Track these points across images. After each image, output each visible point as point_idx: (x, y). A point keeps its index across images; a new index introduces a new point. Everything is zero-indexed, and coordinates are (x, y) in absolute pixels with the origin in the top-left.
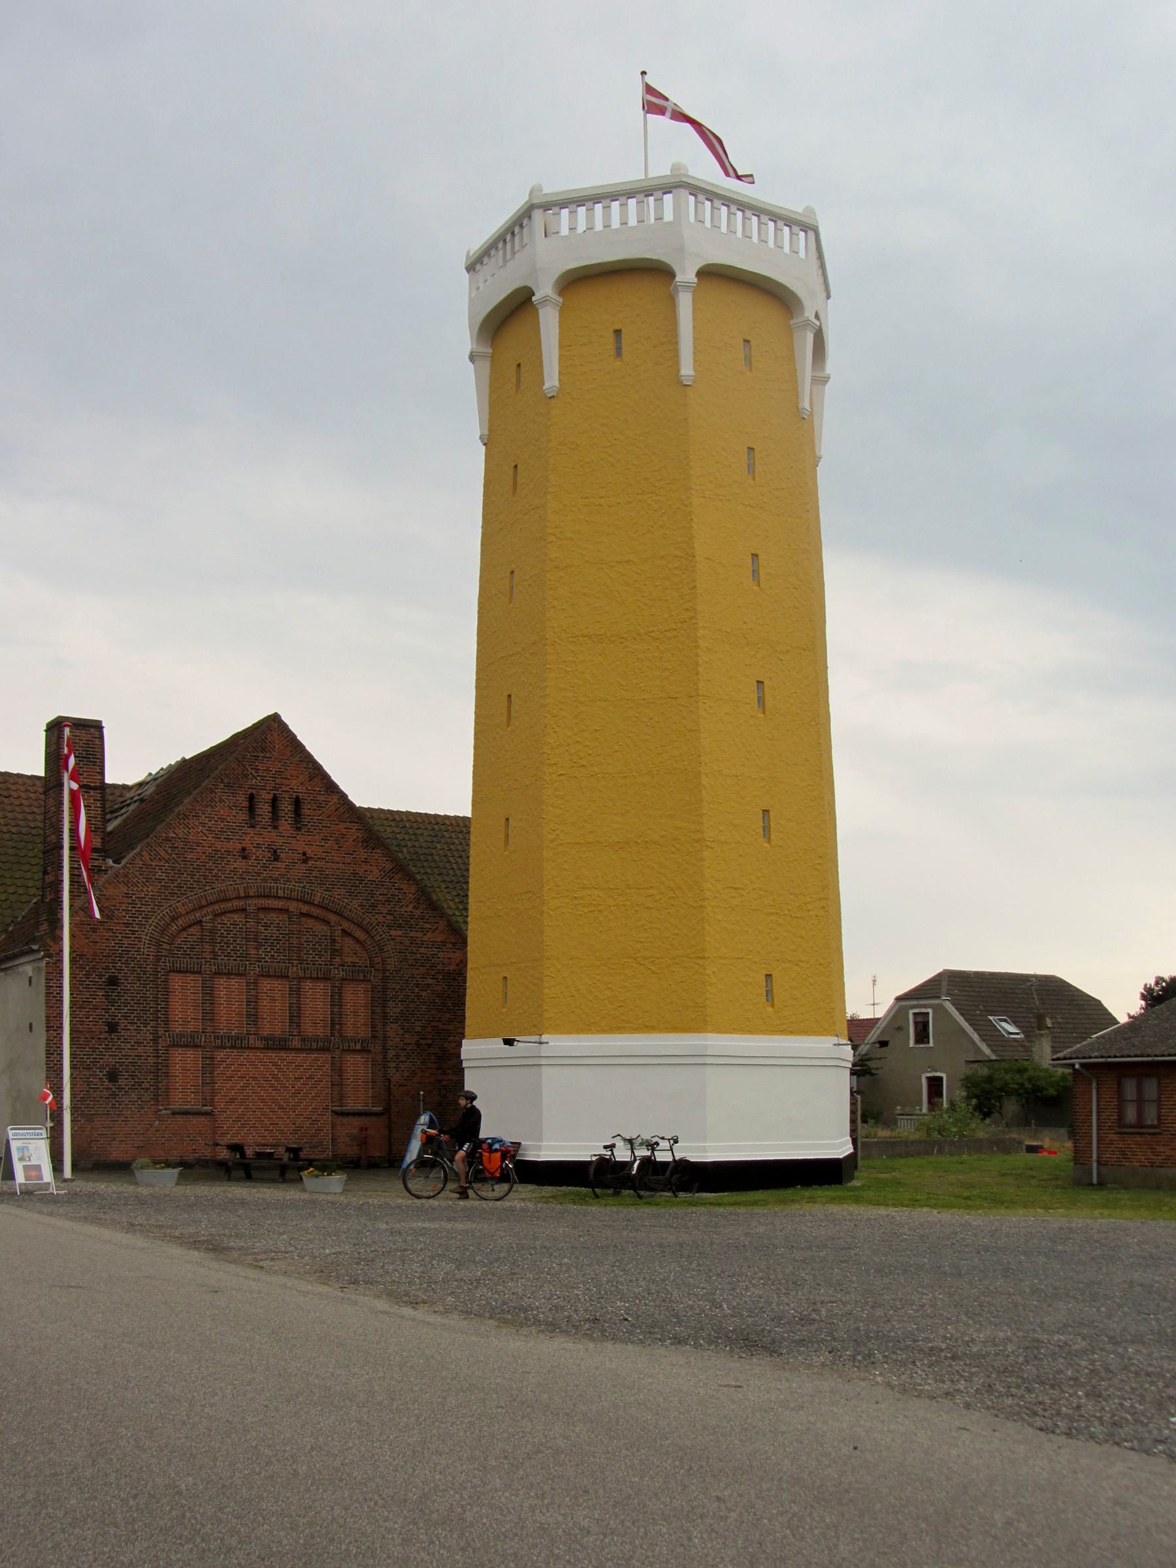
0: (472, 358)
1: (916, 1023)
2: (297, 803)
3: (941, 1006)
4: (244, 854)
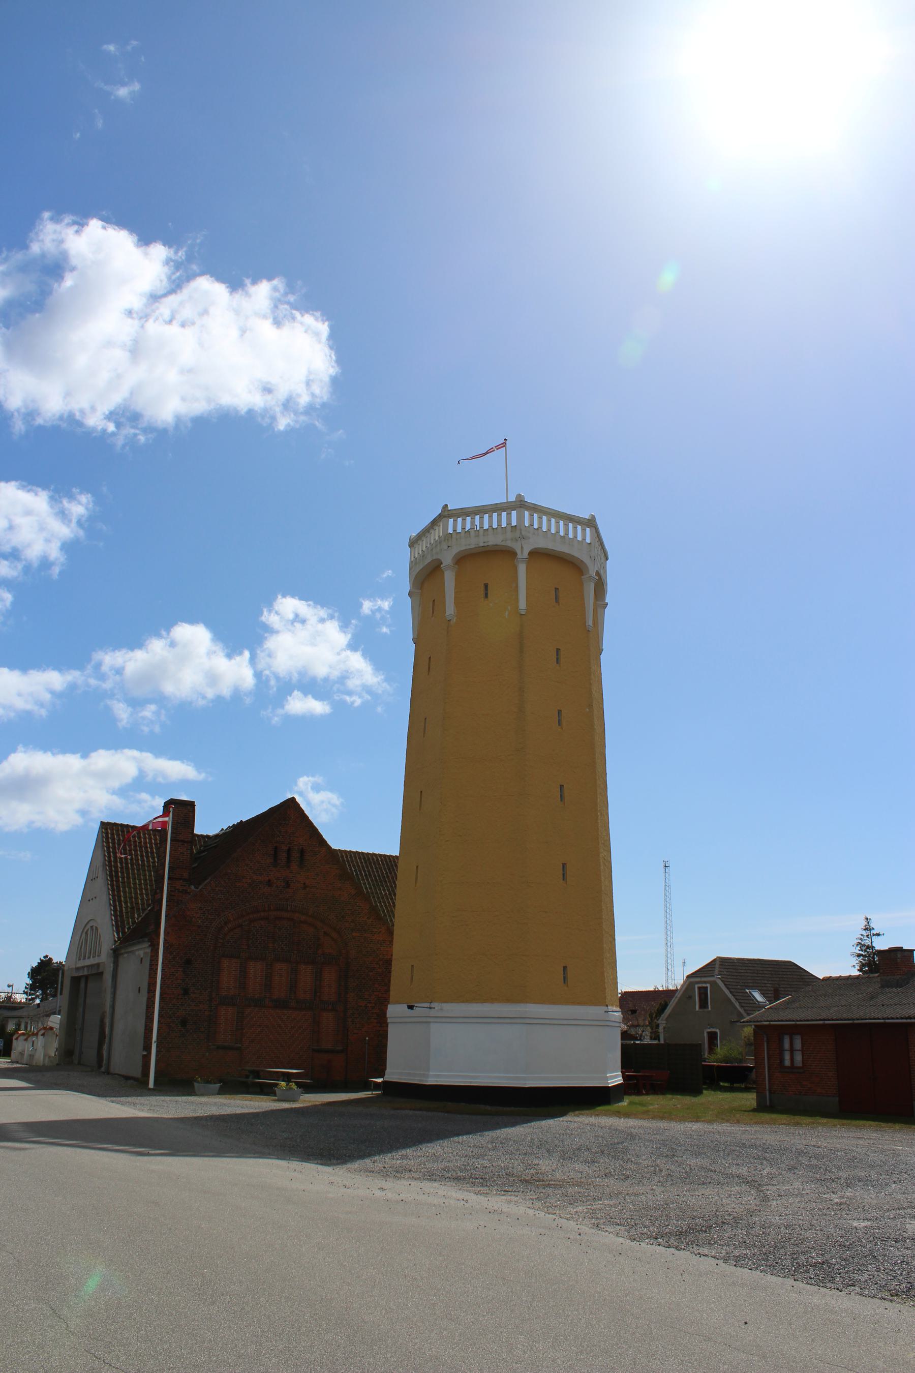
0: (410, 594)
1: (700, 994)
2: (302, 852)
3: (715, 982)
4: (269, 883)
